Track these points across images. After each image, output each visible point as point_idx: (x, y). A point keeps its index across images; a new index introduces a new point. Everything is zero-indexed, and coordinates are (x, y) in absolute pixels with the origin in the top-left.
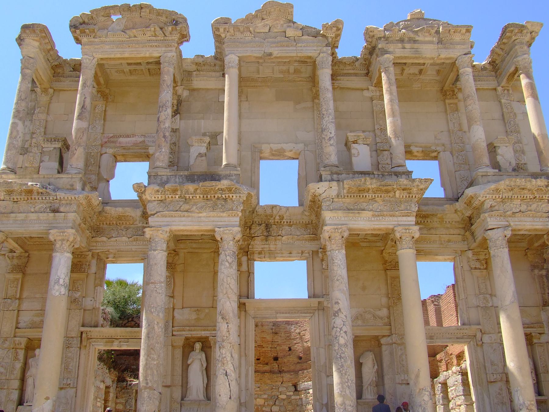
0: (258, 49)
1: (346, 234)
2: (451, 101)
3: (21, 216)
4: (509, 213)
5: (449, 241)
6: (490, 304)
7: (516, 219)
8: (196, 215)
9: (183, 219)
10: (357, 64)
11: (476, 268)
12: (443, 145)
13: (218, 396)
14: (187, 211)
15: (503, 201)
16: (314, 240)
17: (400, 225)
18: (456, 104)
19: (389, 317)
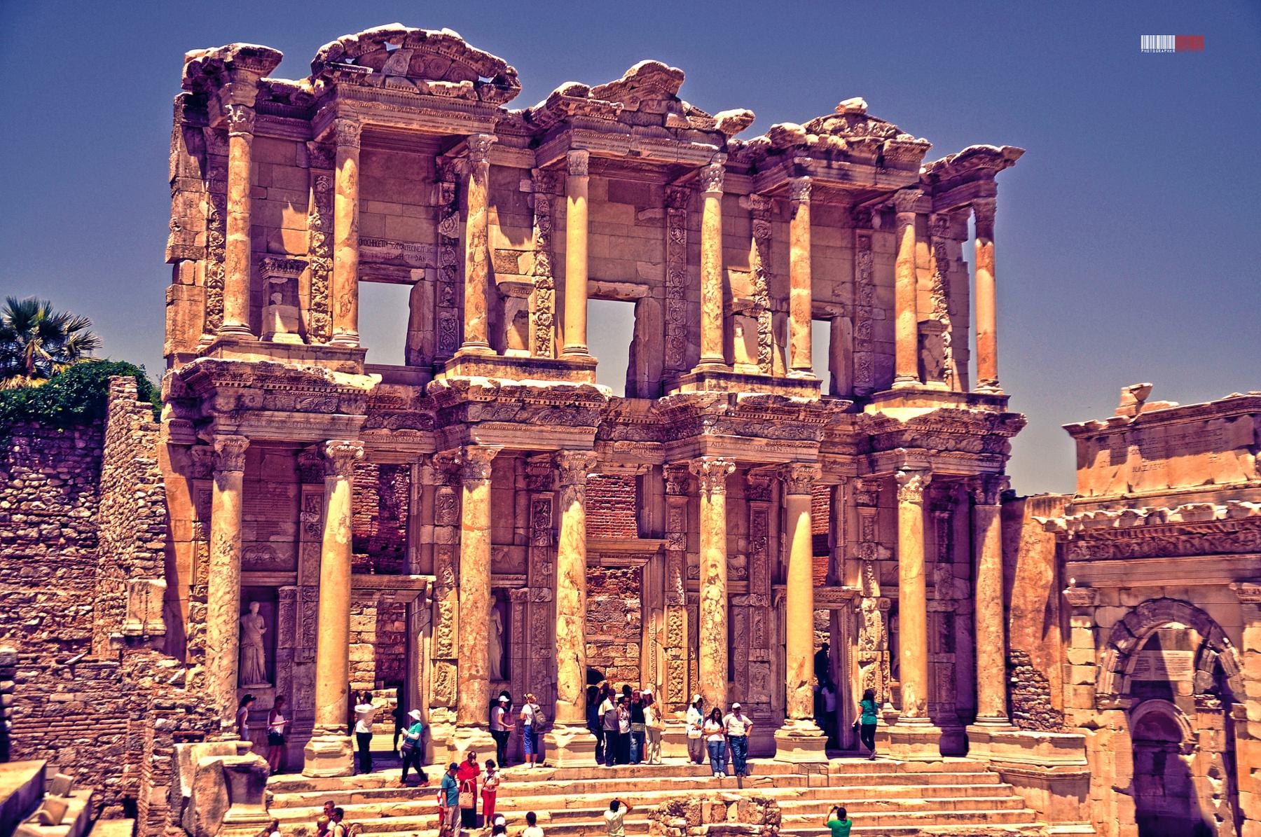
0: (621, 144)
1: (732, 469)
2: (864, 232)
3: (282, 415)
4: (933, 451)
5: (834, 462)
6: (875, 557)
7: (940, 460)
8: (537, 428)
9: (519, 433)
10: (740, 154)
11: (863, 505)
12: (842, 305)
13: (564, 687)
14: (523, 422)
15: (928, 434)
16: (656, 449)
17: (798, 461)
18: (869, 237)
19: (747, 568)
